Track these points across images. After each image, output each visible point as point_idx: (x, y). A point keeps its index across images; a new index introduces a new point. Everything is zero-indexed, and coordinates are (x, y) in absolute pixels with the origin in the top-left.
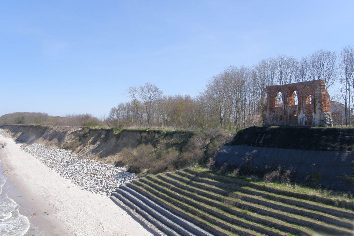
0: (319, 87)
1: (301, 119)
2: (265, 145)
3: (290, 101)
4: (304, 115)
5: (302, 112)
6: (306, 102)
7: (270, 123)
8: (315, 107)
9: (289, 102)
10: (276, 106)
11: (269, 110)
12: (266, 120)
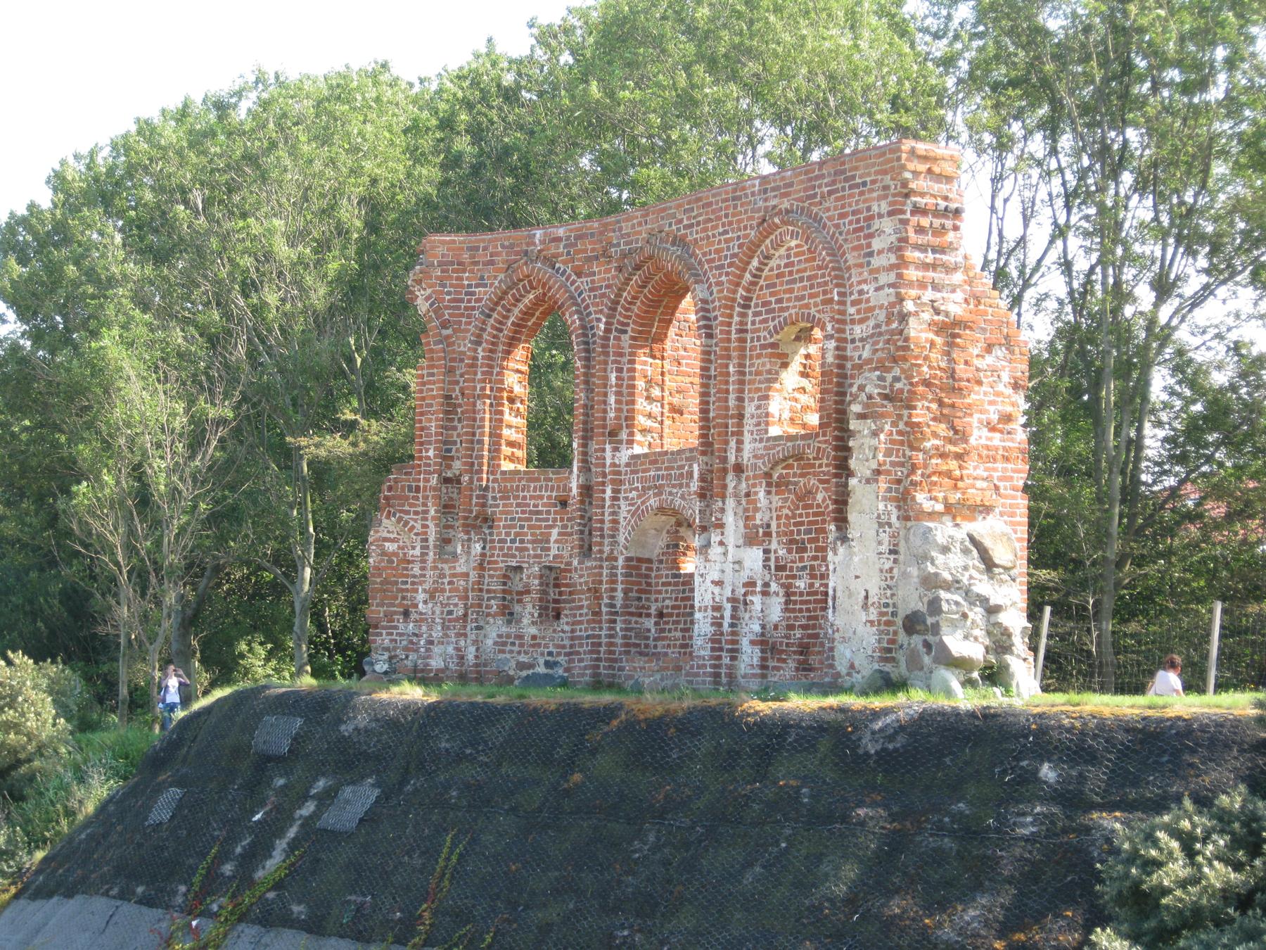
0: (888, 225)
1: (717, 608)
2: (297, 909)
3: (641, 404)
5: (729, 519)
6: (777, 406)
7: (437, 650)
8: (843, 468)
9: (630, 418)
10: (507, 466)
11: (432, 512)
12: (406, 614)
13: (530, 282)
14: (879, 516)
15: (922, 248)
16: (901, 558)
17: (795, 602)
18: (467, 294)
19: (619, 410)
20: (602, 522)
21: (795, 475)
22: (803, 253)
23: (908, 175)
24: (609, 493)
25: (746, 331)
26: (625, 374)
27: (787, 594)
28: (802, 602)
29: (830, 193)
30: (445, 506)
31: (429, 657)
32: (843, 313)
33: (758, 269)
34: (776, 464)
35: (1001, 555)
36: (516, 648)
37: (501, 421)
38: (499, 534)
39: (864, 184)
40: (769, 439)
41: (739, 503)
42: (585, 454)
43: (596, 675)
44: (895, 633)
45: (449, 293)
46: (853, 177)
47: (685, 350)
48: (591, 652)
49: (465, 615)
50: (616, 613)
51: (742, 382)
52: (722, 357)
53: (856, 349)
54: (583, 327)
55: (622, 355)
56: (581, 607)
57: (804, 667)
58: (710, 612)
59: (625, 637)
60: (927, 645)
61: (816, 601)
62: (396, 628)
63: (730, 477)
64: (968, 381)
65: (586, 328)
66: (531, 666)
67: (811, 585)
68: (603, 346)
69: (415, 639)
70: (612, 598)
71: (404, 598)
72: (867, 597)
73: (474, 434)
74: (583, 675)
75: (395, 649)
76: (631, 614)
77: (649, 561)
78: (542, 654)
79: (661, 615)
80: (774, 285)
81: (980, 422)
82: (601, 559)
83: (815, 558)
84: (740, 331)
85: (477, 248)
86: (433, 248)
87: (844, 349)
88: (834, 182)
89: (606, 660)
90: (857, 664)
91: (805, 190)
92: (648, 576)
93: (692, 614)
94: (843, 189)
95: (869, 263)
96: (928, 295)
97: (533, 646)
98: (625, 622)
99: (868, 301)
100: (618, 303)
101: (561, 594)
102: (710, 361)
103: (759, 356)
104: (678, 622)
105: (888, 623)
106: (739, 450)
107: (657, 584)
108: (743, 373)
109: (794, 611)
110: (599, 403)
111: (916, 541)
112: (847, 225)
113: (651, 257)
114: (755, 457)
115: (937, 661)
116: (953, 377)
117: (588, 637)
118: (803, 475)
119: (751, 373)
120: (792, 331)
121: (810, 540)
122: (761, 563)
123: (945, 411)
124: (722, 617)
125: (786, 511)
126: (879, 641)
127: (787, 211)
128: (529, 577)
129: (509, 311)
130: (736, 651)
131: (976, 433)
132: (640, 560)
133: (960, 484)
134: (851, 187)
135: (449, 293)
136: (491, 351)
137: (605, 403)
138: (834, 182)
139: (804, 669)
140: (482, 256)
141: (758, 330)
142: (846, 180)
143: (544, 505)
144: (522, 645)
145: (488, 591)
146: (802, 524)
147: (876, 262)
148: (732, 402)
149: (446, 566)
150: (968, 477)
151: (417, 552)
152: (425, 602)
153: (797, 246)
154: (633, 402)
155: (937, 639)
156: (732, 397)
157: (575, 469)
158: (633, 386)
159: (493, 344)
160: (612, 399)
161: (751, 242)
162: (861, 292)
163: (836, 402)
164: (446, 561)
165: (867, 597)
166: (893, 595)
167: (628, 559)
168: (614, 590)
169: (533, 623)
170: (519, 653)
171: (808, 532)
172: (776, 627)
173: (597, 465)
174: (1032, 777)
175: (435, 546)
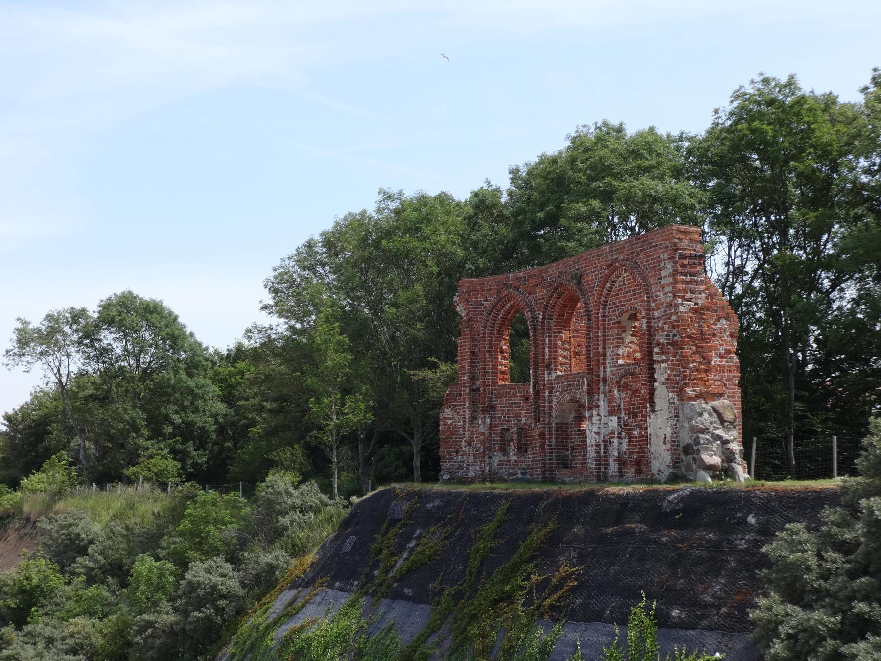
1: (598, 445)
3: (560, 352)
4: (613, 422)
5: (602, 403)
8: (652, 379)
10: (501, 383)
11: (467, 405)
12: (457, 452)
13: (508, 298)
14: (669, 400)
15: (685, 274)
16: (681, 419)
17: (633, 441)
18: (480, 305)
19: (549, 355)
20: (544, 407)
21: (631, 382)
22: (630, 279)
23: (677, 241)
24: (547, 393)
25: (606, 316)
26: (552, 339)
27: (630, 438)
28: (636, 441)
29: (641, 251)
30: (473, 402)
31: (468, 472)
32: (649, 306)
33: (610, 287)
34: (622, 377)
35: (729, 416)
36: (508, 467)
37: (497, 362)
38: (498, 414)
39: (657, 246)
40: (618, 366)
41: (606, 396)
42: (535, 376)
43: (544, 478)
44: (679, 454)
45: (471, 305)
46: (651, 243)
47: (580, 326)
48: (542, 467)
49: (484, 452)
50: (552, 449)
51: (604, 340)
52: (595, 329)
53: (655, 322)
54: (532, 317)
55: (550, 330)
56: (536, 446)
57: (638, 472)
58: (594, 448)
59: (556, 460)
60: (694, 459)
61: (643, 441)
62: (453, 459)
63: (601, 383)
64: (709, 335)
65: (535, 318)
66: (515, 474)
67: (640, 433)
68: (541, 326)
69: (461, 464)
70: (550, 442)
71: (456, 445)
72: (665, 438)
73: (485, 369)
74: (538, 478)
75: (452, 468)
76: (559, 449)
77: (567, 424)
78: (519, 469)
79: (573, 449)
80: (617, 295)
81: (716, 354)
82: (544, 424)
83: (641, 420)
84: (603, 316)
85: (483, 284)
86: (463, 285)
87: (651, 322)
88: (643, 246)
89: (548, 471)
90: (661, 469)
91: (630, 250)
92: (567, 431)
93: (586, 448)
94: (647, 249)
95: (660, 282)
96: (688, 296)
97: (515, 465)
98: (556, 453)
99: (660, 300)
100: (548, 306)
101: (527, 441)
102: (590, 331)
103: (612, 328)
104: (581, 452)
105: (675, 450)
106: (605, 371)
107: (571, 435)
108: (605, 336)
109: (633, 445)
110: (541, 352)
111: (687, 411)
112: (650, 265)
113: (561, 284)
114: (612, 374)
115: (699, 467)
116: (702, 334)
117: (540, 460)
118: (635, 382)
119: (608, 336)
120: (626, 316)
121: (639, 412)
122: (616, 424)
123: (700, 349)
124: (600, 449)
125: (627, 399)
126: (672, 458)
127: (622, 260)
128: (512, 433)
129: (499, 312)
130: (608, 465)
131: (714, 359)
132: (563, 424)
133: (707, 383)
134: (650, 248)
135: (471, 305)
136: (491, 330)
137: (543, 352)
138: (643, 246)
139: (639, 473)
140: (486, 287)
141: (611, 316)
142: (648, 244)
143: (518, 400)
144: (510, 465)
145: (494, 440)
146: (635, 405)
147: (663, 281)
148: (600, 350)
149: (474, 430)
150: (711, 380)
151: (461, 423)
152: (466, 446)
153: (627, 276)
154: (557, 351)
155: (699, 456)
156: (600, 347)
157: (531, 383)
158: (557, 344)
159: (492, 327)
160: (547, 350)
161: (606, 275)
162: (657, 296)
163: (647, 347)
164: (474, 428)
165: (665, 438)
166: (677, 436)
167: (557, 424)
168: (551, 438)
169: (515, 455)
170: (509, 468)
171: (638, 408)
172: (625, 453)
173: (541, 381)
174: (743, 522)
175: (469, 421)
